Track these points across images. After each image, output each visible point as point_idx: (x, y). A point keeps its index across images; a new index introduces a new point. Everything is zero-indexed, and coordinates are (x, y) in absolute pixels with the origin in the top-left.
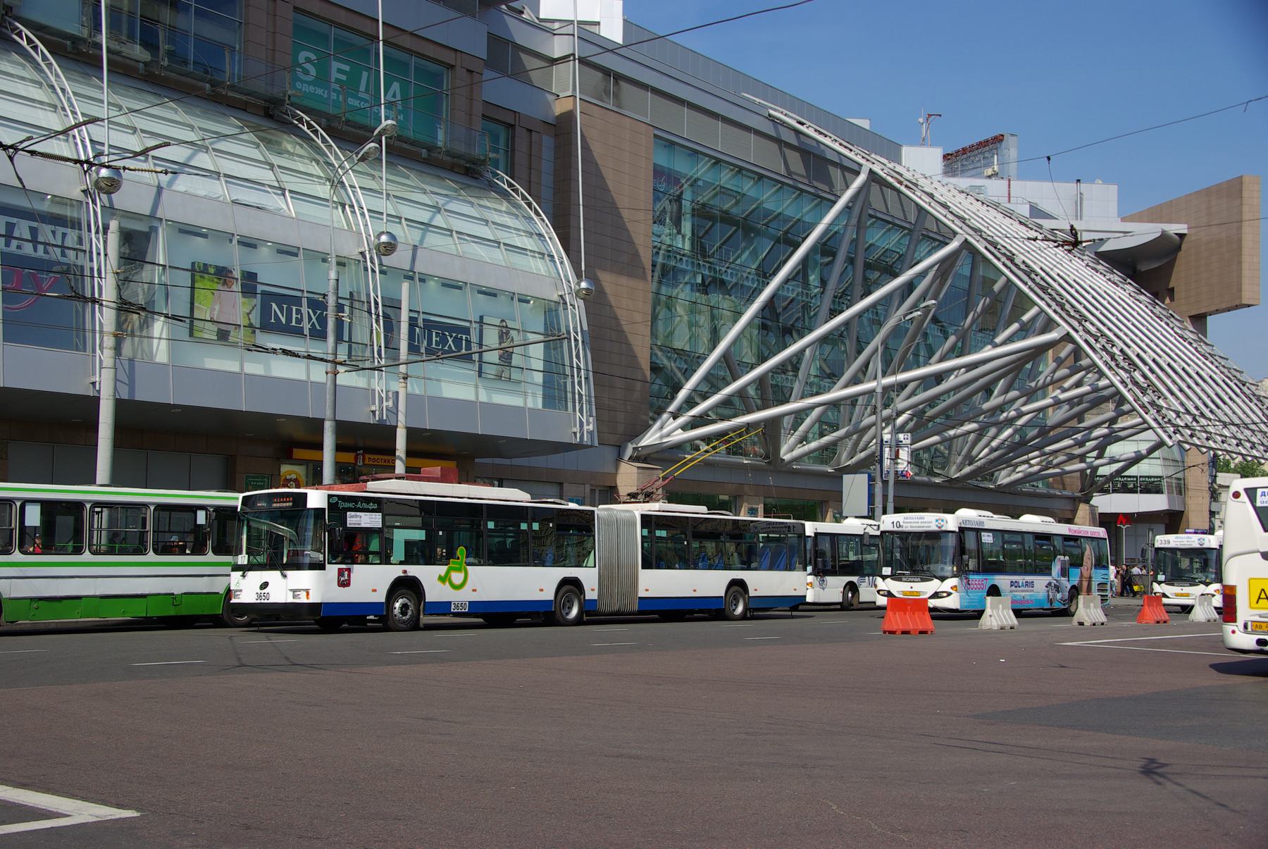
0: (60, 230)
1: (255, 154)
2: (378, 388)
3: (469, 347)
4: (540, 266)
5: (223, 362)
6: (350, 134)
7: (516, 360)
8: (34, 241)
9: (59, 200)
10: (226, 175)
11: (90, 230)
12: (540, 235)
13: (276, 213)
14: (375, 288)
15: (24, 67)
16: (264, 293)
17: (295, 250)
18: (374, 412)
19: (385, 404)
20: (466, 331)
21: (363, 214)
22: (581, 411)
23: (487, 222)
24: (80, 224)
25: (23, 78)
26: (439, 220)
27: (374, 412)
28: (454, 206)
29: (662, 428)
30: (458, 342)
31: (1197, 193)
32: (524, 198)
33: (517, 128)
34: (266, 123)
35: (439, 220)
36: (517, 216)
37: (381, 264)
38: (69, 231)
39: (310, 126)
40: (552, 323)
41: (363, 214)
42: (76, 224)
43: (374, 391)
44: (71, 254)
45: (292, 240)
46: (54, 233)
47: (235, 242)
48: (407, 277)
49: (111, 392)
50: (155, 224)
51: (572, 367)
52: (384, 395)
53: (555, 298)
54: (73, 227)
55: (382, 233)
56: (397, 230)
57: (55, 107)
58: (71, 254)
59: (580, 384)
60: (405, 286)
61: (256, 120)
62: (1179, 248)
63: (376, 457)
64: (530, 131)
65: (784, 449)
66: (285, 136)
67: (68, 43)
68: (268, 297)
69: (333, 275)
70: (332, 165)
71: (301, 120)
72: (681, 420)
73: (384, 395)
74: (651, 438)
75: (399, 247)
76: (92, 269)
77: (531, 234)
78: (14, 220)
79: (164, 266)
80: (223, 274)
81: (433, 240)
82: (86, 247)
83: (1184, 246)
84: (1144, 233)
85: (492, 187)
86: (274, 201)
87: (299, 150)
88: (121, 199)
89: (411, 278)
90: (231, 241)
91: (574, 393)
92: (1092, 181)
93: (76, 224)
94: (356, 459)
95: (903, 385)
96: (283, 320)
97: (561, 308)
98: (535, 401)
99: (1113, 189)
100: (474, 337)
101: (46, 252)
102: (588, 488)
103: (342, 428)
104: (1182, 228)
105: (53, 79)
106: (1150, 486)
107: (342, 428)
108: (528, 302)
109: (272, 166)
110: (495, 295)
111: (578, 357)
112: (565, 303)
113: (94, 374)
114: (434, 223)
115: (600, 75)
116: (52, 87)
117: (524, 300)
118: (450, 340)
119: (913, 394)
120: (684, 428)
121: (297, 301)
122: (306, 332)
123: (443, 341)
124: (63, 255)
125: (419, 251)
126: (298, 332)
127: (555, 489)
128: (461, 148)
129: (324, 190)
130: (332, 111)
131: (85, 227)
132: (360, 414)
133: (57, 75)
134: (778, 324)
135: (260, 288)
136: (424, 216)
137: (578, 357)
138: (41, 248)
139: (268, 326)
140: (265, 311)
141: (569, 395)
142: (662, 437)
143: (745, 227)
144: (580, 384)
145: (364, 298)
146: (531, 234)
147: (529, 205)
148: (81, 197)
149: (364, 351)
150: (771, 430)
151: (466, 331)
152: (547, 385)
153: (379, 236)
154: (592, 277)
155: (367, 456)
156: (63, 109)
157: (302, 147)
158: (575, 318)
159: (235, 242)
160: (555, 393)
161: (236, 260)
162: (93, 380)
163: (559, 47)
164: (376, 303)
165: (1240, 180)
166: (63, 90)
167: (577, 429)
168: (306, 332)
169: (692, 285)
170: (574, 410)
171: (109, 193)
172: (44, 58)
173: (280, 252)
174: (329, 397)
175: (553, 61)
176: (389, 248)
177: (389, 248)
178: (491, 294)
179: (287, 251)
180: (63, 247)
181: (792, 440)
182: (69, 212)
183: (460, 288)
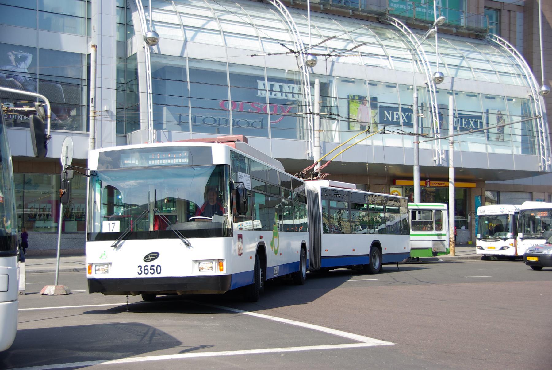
0: (292, 85)
1: (373, 40)
2: (437, 149)
3: (482, 126)
4: (518, 81)
5: (363, 140)
6: (419, 26)
7: (507, 130)
8: (281, 92)
9: (291, 72)
10: (499, 72)
11: (304, 84)
12: (518, 65)
13: (385, 68)
14: (434, 101)
15: (274, 14)
16: (381, 107)
17: (394, 85)
18: (435, 161)
19: (441, 156)
20: (480, 117)
21: (426, 64)
22: (544, 154)
23: (489, 61)
24: (300, 82)
25: (274, 20)
26: (464, 64)
27: (435, 161)
28: (471, 55)
30: (476, 123)
32: (509, 47)
33: (503, 11)
34: (379, 25)
36: (504, 57)
37: (436, 88)
38: (295, 86)
39: (399, 24)
41: (426, 64)
42: (298, 82)
43: (435, 150)
44: (296, 96)
45: (393, 80)
46: (289, 87)
47: (367, 84)
50: (331, 79)
51: (538, 132)
52: (440, 152)
53: (527, 96)
54: (297, 84)
56: (444, 70)
57: (288, 30)
58: (296, 96)
59: (542, 140)
60: (451, 98)
61: (374, 25)
63: (435, 182)
64: (509, 11)
66: (387, 31)
67: (351, 11)
69: (415, 95)
70: (410, 42)
71: (394, 22)
73: (440, 152)
76: (306, 102)
77: (513, 65)
78: (272, 83)
80: (362, 99)
81: (463, 74)
82: (302, 92)
85: (490, 43)
86: (383, 62)
87: (393, 36)
90: (365, 83)
91: (539, 145)
93: (298, 82)
94: (426, 183)
96: (390, 119)
97: (531, 101)
98: (518, 150)
100: (484, 120)
101: (286, 96)
102: (547, 194)
103: (422, 169)
105: (286, 18)
107: (422, 169)
108: (512, 100)
109: (382, 46)
110: (494, 98)
111: (541, 126)
112: (533, 99)
113: (308, 150)
114: (462, 65)
116: (286, 22)
117: (510, 100)
118: (472, 123)
121: (396, 109)
123: (468, 123)
124: (293, 96)
125: (455, 80)
126: (398, 124)
127: (528, 195)
128: (473, 25)
129: (408, 55)
130: (407, 15)
131: (301, 83)
132: (429, 162)
133: (288, 16)
135: (379, 105)
136: (456, 62)
137: (541, 126)
138: (284, 94)
139: (384, 122)
140: (382, 115)
141: (537, 147)
144: (542, 140)
145: (428, 105)
146: (513, 65)
147: (511, 50)
149: (429, 131)
151: (480, 117)
152: (524, 142)
153: (435, 74)
154: (547, 84)
155: (431, 182)
156: (291, 31)
157: (395, 34)
159: (367, 84)
161: (367, 92)
162: (308, 152)
164: (435, 108)
166: (291, 22)
167: (541, 164)
170: (540, 154)
171: (311, 67)
172: (283, 9)
174: (415, 154)
176: (440, 80)
177: (440, 80)
178: (492, 98)
179: (391, 86)
180: (293, 93)
182: (295, 77)
183: (476, 96)
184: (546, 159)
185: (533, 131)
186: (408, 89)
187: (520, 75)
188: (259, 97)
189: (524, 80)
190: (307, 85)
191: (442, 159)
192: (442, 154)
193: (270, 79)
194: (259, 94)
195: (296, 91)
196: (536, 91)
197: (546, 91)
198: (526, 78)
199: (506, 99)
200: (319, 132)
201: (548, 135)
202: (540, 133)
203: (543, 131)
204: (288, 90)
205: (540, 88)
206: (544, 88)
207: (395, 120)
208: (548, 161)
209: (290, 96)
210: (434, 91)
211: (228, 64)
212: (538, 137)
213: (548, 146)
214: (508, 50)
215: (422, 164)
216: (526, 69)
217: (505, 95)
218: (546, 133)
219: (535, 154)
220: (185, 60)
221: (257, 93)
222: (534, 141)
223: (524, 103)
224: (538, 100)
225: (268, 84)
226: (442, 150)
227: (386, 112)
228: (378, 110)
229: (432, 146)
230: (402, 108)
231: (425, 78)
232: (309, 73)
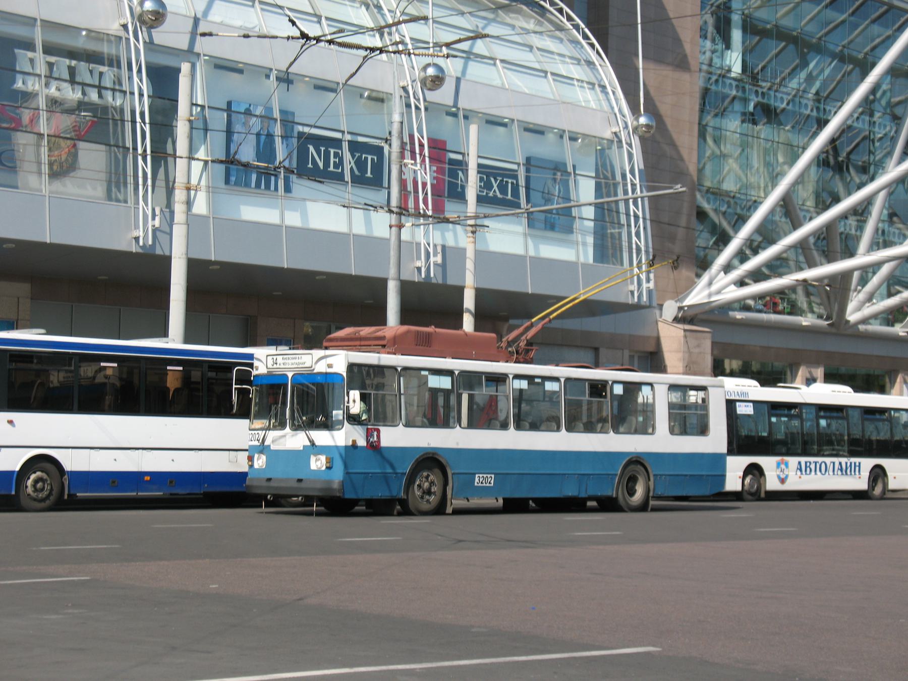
2: (423, 242)
3: (515, 193)
4: (587, 97)
5: (257, 211)
8: (72, 81)
9: (95, 35)
11: (130, 68)
12: (590, 63)
16: (301, 135)
17: (334, 86)
18: (419, 269)
19: (432, 259)
20: (513, 175)
23: (531, 48)
27: (419, 269)
28: (492, 30)
29: (710, 284)
30: (503, 188)
32: (569, 19)
35: (480, 47)
36: (561, 40)
37: (425, 100)
38: (104, 69)
40: (604, 165)
42: (114, 62)
43: (418, 244)
44: (108, 95)
46: (91, 72)
47: (273, 77)
48: (449, 114)
49: (184, 250)
51: (628, 215)
53: (608, 134)
54: (111, 65)
55: (428, 65)
58: (108, 95)
59: (638, 235)
65: (851, 306)
68: (306, 140)
69: (396, 118)
72: (735, 274)
73: (431, 250)
74: (697, 296)
75: (447, 80)
76: (133, 112)
77: (579, 61)
78: (52, 59)
79: (203, 107)
81: (476, 70)
88: (161, 36)
89: (455, 115)
90: (268, 77)
93: (114, 62)
96: (321, 165)
97: (615, 146)
98: (587, 254)
102: (627, 353)
107: (406, 287)
112: (620, 141)
113: (137, 227)
120: (741, 283)
121: (337, 143)
122: (348, 177)
124: (100, 96)
126: (339, 178)
127: (589, 356)
134: (844, 162)
139: (305, 170)
140: (303, 154)
142: (710, 295)
143: (802, 46)
144: (638, 235)
146: (579, 61)
147: (577, 27)
148: (122, 33)
150: (838, 288)
151: (513, 175)
153: (425, 68)
154: (652, 110)
158: (630, 160)
159: (273, 77)
160: (607, 249)
162: (135, 234)
164: (421, 145)
167: (634, 287)
168: (348, 177)
169: (744, 114)
170: (631, 264)
171: (151, 27)
173: (317, 87)
174: (393, 253)
176: (437, 81)
177: (437, 81)
178: (538, 131)
179: (323, 87)
181: (862, 296)
182: (105, 49)
183: (505, 125)
184: (643, 277)
185: (618, 212)
186: (361, 96)
187: (593, 84)
189: (601, 96)
190: (139, 71)
191: (436, 264)
192: (435, 255)
193: (49, 50)
194: (19, 85)
195: (107, 82)
196: (626, 123)
197: (647, 126)
198: (607, 94)
199: (566, 137)
200: (188, 189)
201: (648, 223)
202: (632, 219)
203: (640, 214)
204: (88, 80)
205: (637, 119)
206: (643, 120)
207: (331, 168)
208: (648, 280)
209: (94, 96)
210: (422, 107)
212: (629, 225)
213: (647, 246)
214: (568, 25)
215: (405, 276)
216: (607, 73)
217: (566, 127)
218: (644, 219)
219: (622, 264)
221: (14, 82)
222: (620, 234)
223: (602, 150)
224: (630, 145)
225: (41, 59)
226: (435, 246)
227: (311, 149)
228: (295, 141)
229: (413, 235)
230: (350, 142)
231: (402, 75)
232: (145, 42)
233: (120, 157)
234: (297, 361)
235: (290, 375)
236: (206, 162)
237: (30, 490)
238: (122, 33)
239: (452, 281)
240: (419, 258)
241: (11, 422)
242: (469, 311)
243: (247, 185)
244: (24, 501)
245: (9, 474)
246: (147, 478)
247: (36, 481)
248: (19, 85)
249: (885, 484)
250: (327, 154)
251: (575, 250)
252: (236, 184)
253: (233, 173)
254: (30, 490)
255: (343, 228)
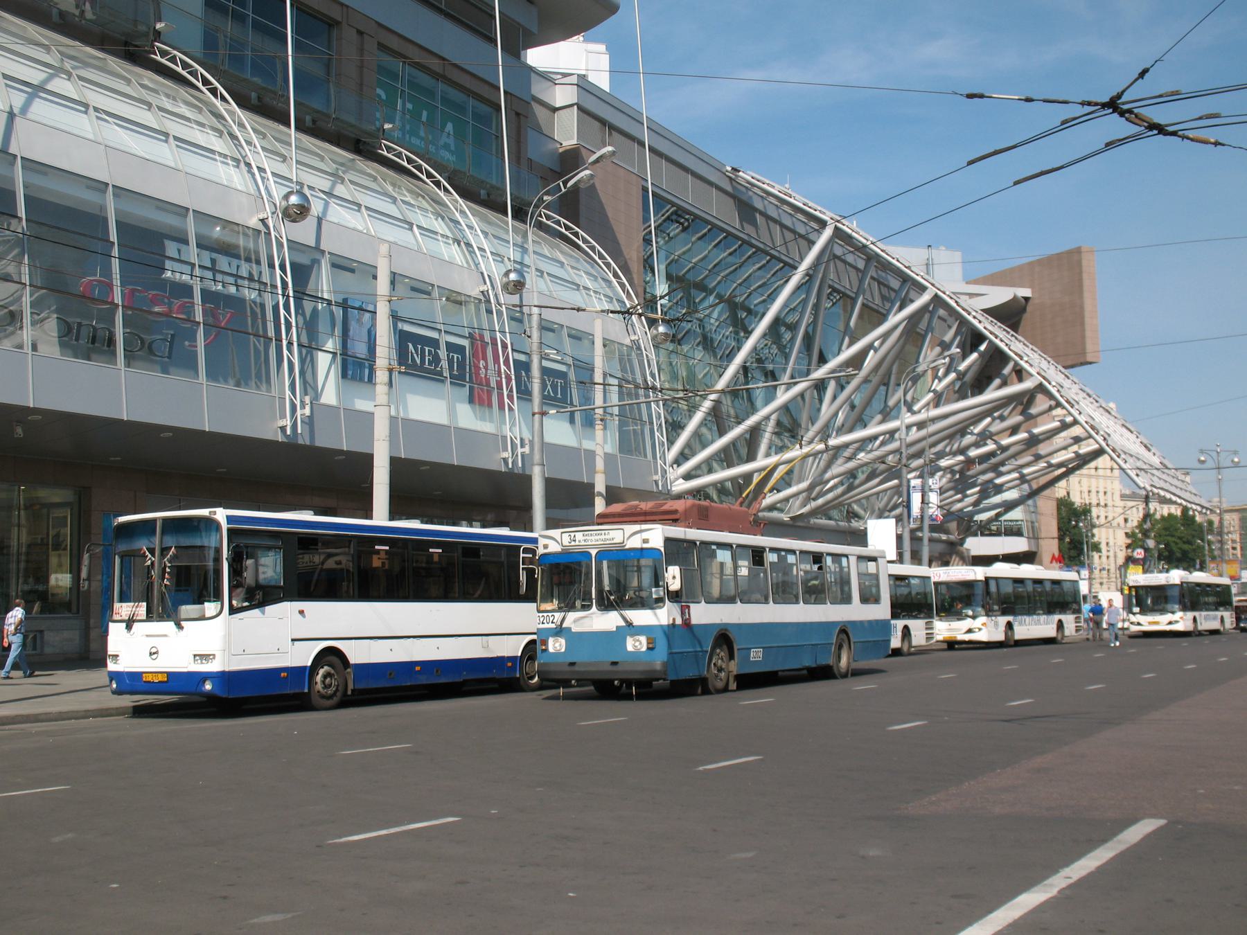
0: (235, 262)
2: (509, 434)
18: (505, 460)
30: (554, 387)
31: (1039, 261)
42: (252, 258)
50: (317, 256)
52: (518, 442)
53: (627, 341)
54: (248, 260)
57: (221, 133)
62: (1024, 310)
79: (329, 303)
83: (1029, 309)
84: (1000, 295)
92: (937, 248)
95: (875, 437)
96: (418, 361)
99: (957, 256)
104: (1026, 292)
106: (1014, 531)
110: (579, 339)
113: (283, 416)
115: (597, 124)
119: (883, 444)
121: (434, 343)
122: (446, 374)
151: (563, 375)
153: (507, 274)
162: (281, 423)
163: (563, 96)
165: (1078, 251)
167: (658, 477)
168: (446, 374)
173: (414, 289)
175: (555, 110)
183: (553, 331)
188: (166, 280)
211: (110, 188)
219: (645, 456)
220: (13, 163)
233: (262, 349)
234: (603, 537)
235: (594, 552)
236: (334, 354)
237: (319, 687)
238: (261, 227)
239: (527, 473)
240: (505, 449)
241: (301, 612)
242: (600, 494)
243: (361, 380)
244: (316, 700)
245: (301, 670)
246: (418, 668)
247: (325, 677)
248: (169, 274)
249: (910, 642)
250: (423, 351)
251: (602, 442)
252: (354, 378)
253: (350, 367)
254: (319, 687)
255: (443, 420)
